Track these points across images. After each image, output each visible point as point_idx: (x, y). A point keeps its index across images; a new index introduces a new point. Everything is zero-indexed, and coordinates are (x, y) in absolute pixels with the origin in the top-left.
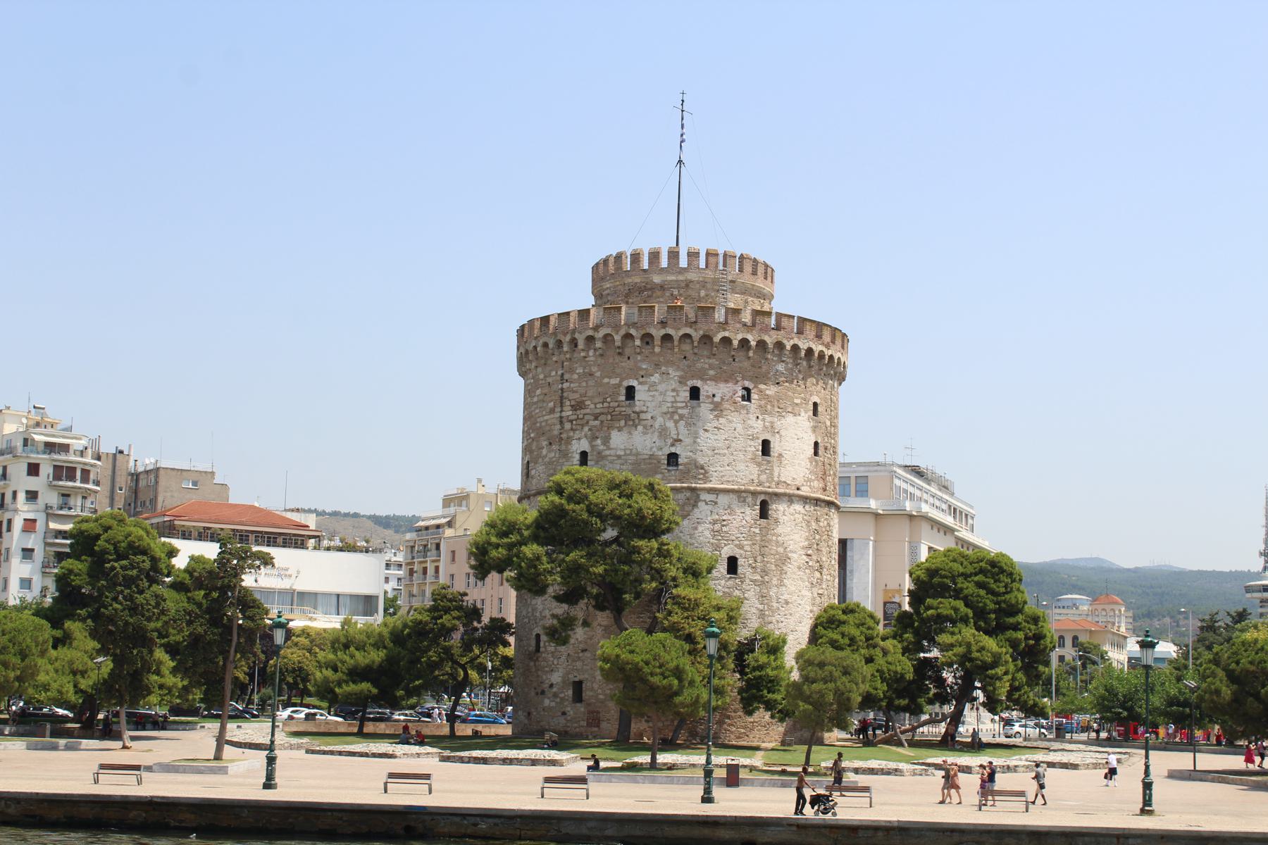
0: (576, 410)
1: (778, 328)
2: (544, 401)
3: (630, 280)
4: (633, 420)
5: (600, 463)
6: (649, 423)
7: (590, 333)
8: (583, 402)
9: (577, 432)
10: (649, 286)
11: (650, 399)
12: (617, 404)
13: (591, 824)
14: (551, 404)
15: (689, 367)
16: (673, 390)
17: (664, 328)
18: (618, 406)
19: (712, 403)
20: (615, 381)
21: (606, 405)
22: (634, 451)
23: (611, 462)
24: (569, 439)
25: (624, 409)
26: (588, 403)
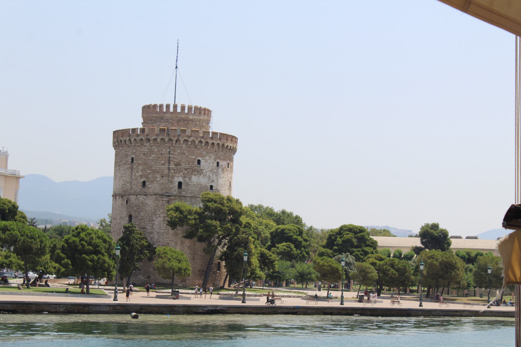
0: (176, 166)
1: (220, 139)
2: (158, 160)
3: (180, 116)
4: (200, 172)
5: (188, 187)
6: (205, 174)
7: (186, 138)
8: (180, 163)
9: (177, 174)
10: (187, 119)
11: (205, 165)
12: (194, 166)
13: (438, 312)
14: (163, 162)
15: (217, 155)
16: (212, 163)
17: (213, 140)
18: (195, 166)
19: (222, 168)
20: (194, 157)
21: (190, 165)
22: (200, 184)
23: (192, 187)
24: (173, 177)
25: (197, 168)
26: (182, 164)
